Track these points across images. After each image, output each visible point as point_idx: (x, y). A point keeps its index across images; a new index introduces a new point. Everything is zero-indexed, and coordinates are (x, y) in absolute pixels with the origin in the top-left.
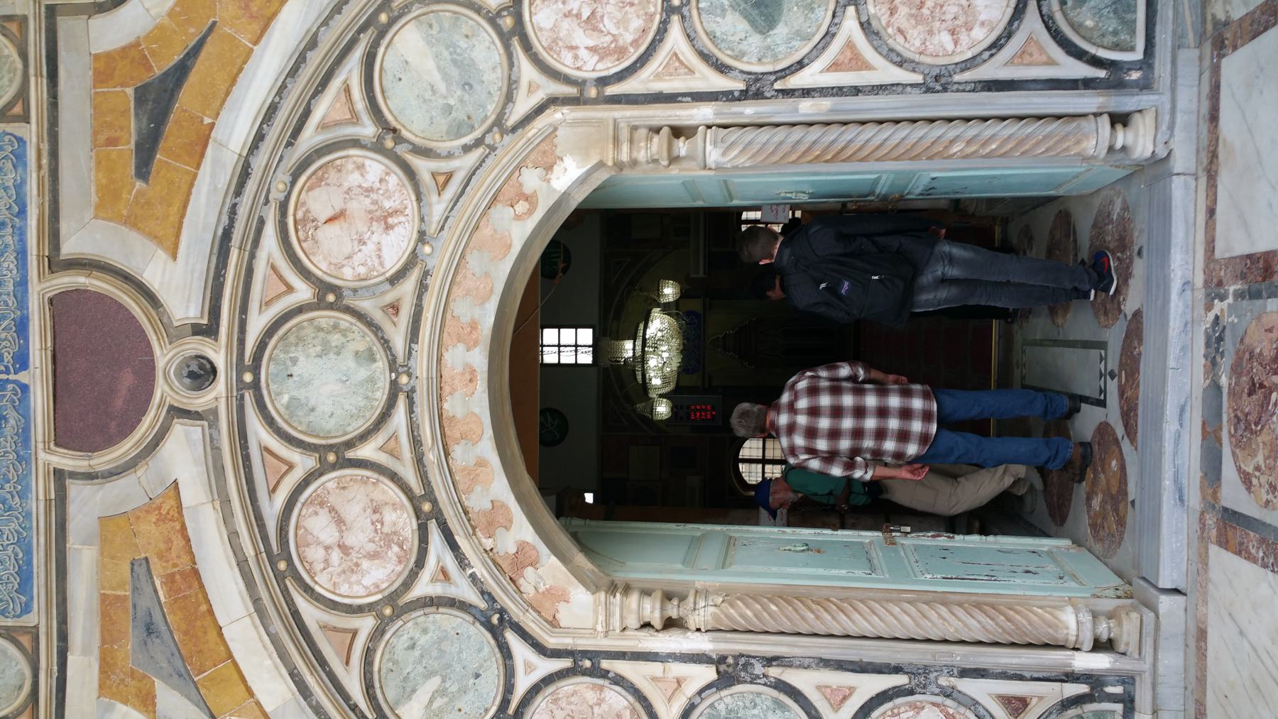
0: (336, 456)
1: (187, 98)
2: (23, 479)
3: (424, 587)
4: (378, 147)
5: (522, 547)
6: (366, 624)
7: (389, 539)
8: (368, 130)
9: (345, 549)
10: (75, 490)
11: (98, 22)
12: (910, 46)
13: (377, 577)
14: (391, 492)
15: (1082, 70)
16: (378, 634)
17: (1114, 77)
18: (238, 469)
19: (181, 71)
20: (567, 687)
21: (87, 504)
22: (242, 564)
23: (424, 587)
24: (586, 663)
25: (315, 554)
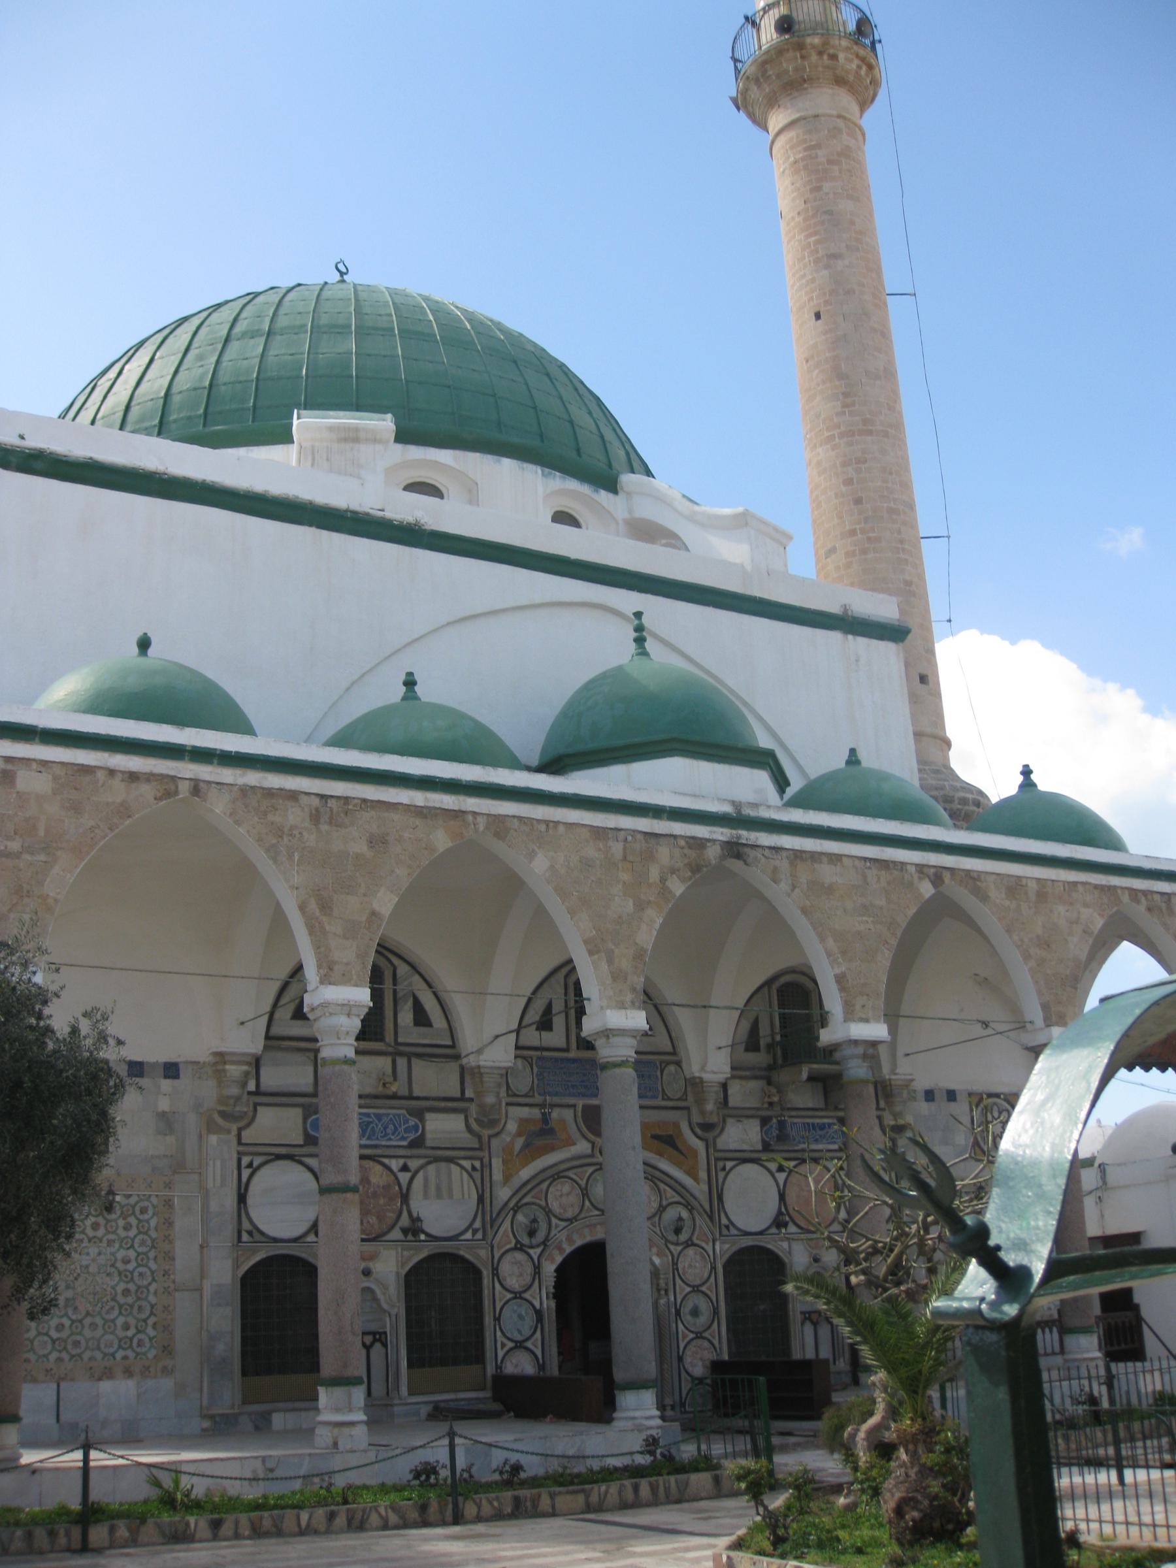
0: (585, 1193)
1: (670, 1150)
2: (573, 1095)
3: (554, 1221)
4: (660, 1205)
5: (564, 1250)
6: (543, 1203)
7: (565, 1210)
8: (664, 1203)
9: (561, 1196)
10: (571, 1111)
11: (686, 1123)
12: (688, 1352)
13: (555, 1206)
14: (577, 1210)
15: (684, 1395)
16: (540, 1206)
17: (683, 1405)
18: (580, 1162)
19: (677, 1149)
20: (530, 1264)
21: (568, 1114)
22: (555, 1165)
23: (554, 1221)
24: (537, 1269)
25: (559, 1187)
